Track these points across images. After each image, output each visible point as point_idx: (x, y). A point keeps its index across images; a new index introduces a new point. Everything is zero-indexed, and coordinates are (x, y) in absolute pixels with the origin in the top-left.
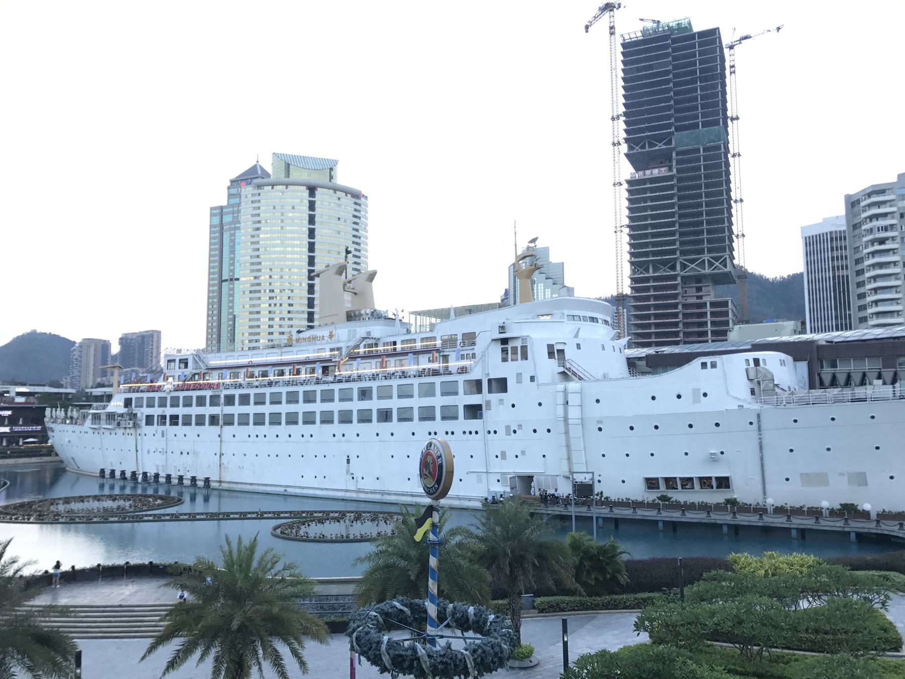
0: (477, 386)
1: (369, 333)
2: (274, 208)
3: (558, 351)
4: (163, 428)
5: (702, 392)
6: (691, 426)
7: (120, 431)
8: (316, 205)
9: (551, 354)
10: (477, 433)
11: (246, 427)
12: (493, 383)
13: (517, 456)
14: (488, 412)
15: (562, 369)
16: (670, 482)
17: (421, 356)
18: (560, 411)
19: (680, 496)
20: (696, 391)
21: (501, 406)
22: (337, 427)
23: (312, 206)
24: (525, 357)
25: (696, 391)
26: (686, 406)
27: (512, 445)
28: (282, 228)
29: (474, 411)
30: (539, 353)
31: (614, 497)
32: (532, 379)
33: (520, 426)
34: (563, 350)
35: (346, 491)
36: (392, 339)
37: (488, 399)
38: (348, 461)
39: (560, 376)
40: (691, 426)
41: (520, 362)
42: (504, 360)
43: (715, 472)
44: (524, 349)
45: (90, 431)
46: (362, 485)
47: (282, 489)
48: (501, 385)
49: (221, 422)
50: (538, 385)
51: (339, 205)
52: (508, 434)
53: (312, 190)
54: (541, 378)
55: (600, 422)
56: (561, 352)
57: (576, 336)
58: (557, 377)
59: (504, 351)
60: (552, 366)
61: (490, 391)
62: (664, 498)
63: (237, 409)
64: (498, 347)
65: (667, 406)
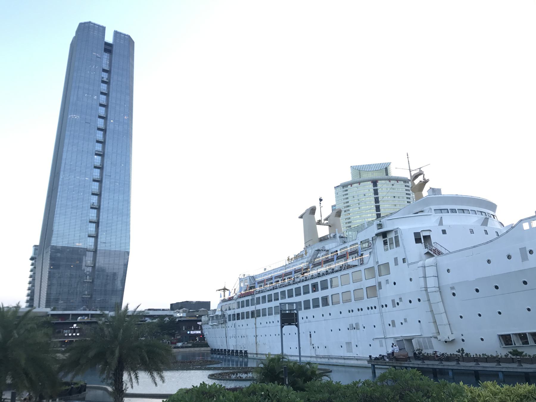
1: (323, 247)
2: (354, 197)
3: (424, 237)
5: (528, 249)
6: (525, 283)
7: (220, 326)
8: (379, 191)
10: (375, 308)
12: (382, 267)
13: (402, 323)
14: (380, 290)
15: (426, 250)
16: (523, 337)
20: (522, 250)
21: (388, 285)
23: (376, 192)
24: (397, 245)
25: (522, 250)
27: (396, 314)
28: (359, 208)
29: (373, 291)
31: (472, 354)
32: (404, 260)
33: (400, 299)
34: (429, 236)
35: (311, 357)
36: (335, 250)
37: (379, 281)
39: (426, 255)
40: (525, 283)
41: (395, 249)
49: (255, 316)
50: (408, 265)
51: (393, 189)
52: (394, 306)
53: (375, 183)
54: (410, 260)
55: (453, 288)
56: (427, 238)
57: (441, 223)
58: (424, 257)
59: (385, 243)
60: (421, 248)
62: (515, 353)
63: (260, 307)
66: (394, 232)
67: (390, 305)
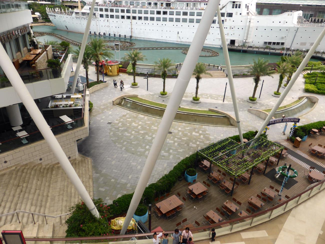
0: (223, 15)
4: (107, 19)
9: (246, 7)
11: (118, 19)
16: (270, 43)
17: (202, 3)
18: (248, 24)
19: (272, 46)
22: (174, 23)
24: (239, 7)
26: (281, 25)
30: (243, 6)
32: (241, 14)
33: (234, 27)
38: (178, 33)
42: (233, 7)
43: (281, 41)
44: (240, 5)
45: (75, 18)
46: (182, 40)
47: (155, 40)
48: (230, 15)
50: (242, 16)
52: (230, 29)
54: (242, 14)
56: (248, 6)
59: (233, 5)
61: (227, 16)
64: (232, 4)
65: (277, 24)
66: (239, 2)
67: (229, 28)
